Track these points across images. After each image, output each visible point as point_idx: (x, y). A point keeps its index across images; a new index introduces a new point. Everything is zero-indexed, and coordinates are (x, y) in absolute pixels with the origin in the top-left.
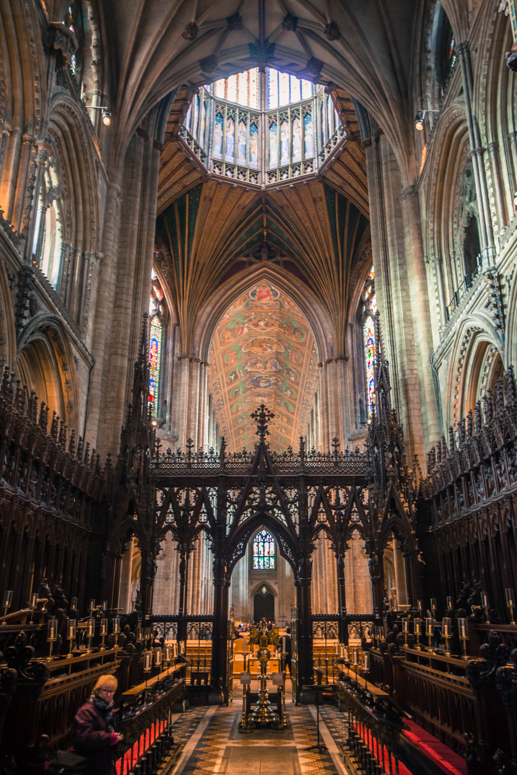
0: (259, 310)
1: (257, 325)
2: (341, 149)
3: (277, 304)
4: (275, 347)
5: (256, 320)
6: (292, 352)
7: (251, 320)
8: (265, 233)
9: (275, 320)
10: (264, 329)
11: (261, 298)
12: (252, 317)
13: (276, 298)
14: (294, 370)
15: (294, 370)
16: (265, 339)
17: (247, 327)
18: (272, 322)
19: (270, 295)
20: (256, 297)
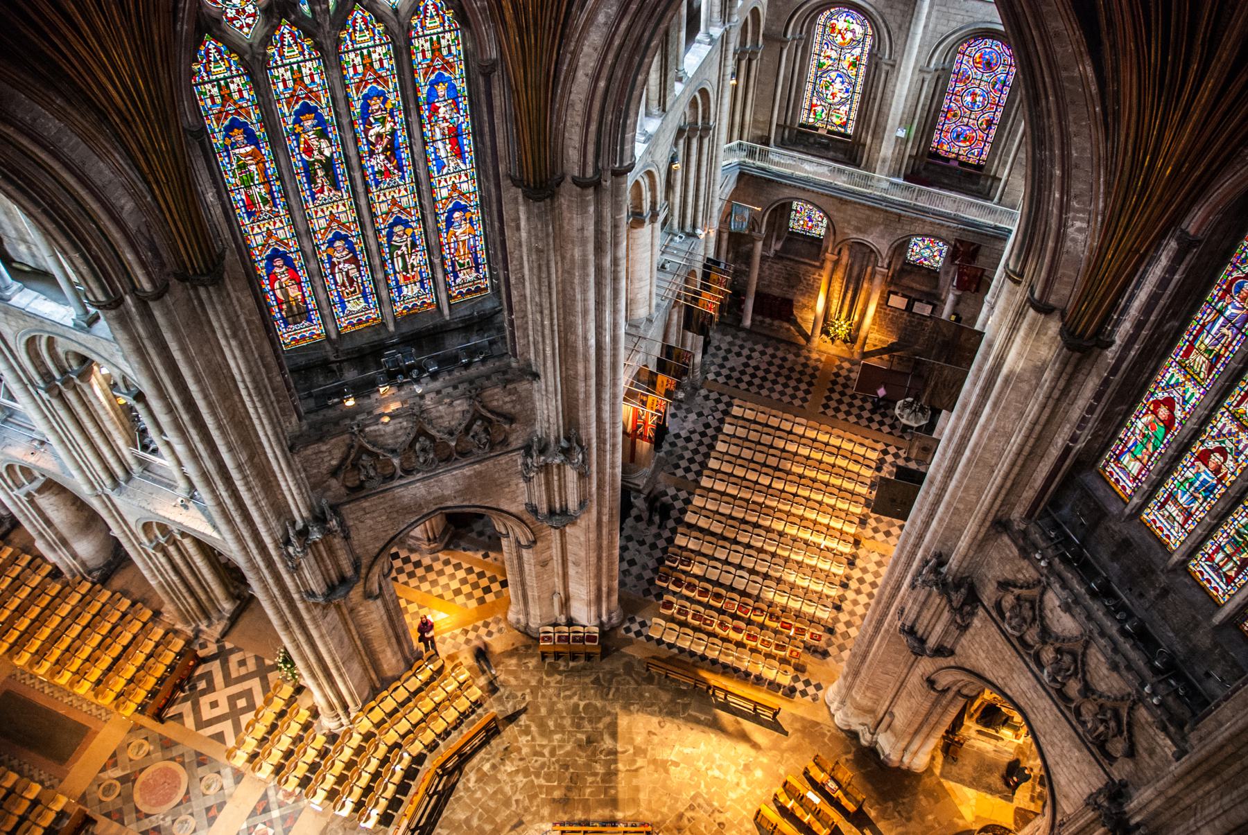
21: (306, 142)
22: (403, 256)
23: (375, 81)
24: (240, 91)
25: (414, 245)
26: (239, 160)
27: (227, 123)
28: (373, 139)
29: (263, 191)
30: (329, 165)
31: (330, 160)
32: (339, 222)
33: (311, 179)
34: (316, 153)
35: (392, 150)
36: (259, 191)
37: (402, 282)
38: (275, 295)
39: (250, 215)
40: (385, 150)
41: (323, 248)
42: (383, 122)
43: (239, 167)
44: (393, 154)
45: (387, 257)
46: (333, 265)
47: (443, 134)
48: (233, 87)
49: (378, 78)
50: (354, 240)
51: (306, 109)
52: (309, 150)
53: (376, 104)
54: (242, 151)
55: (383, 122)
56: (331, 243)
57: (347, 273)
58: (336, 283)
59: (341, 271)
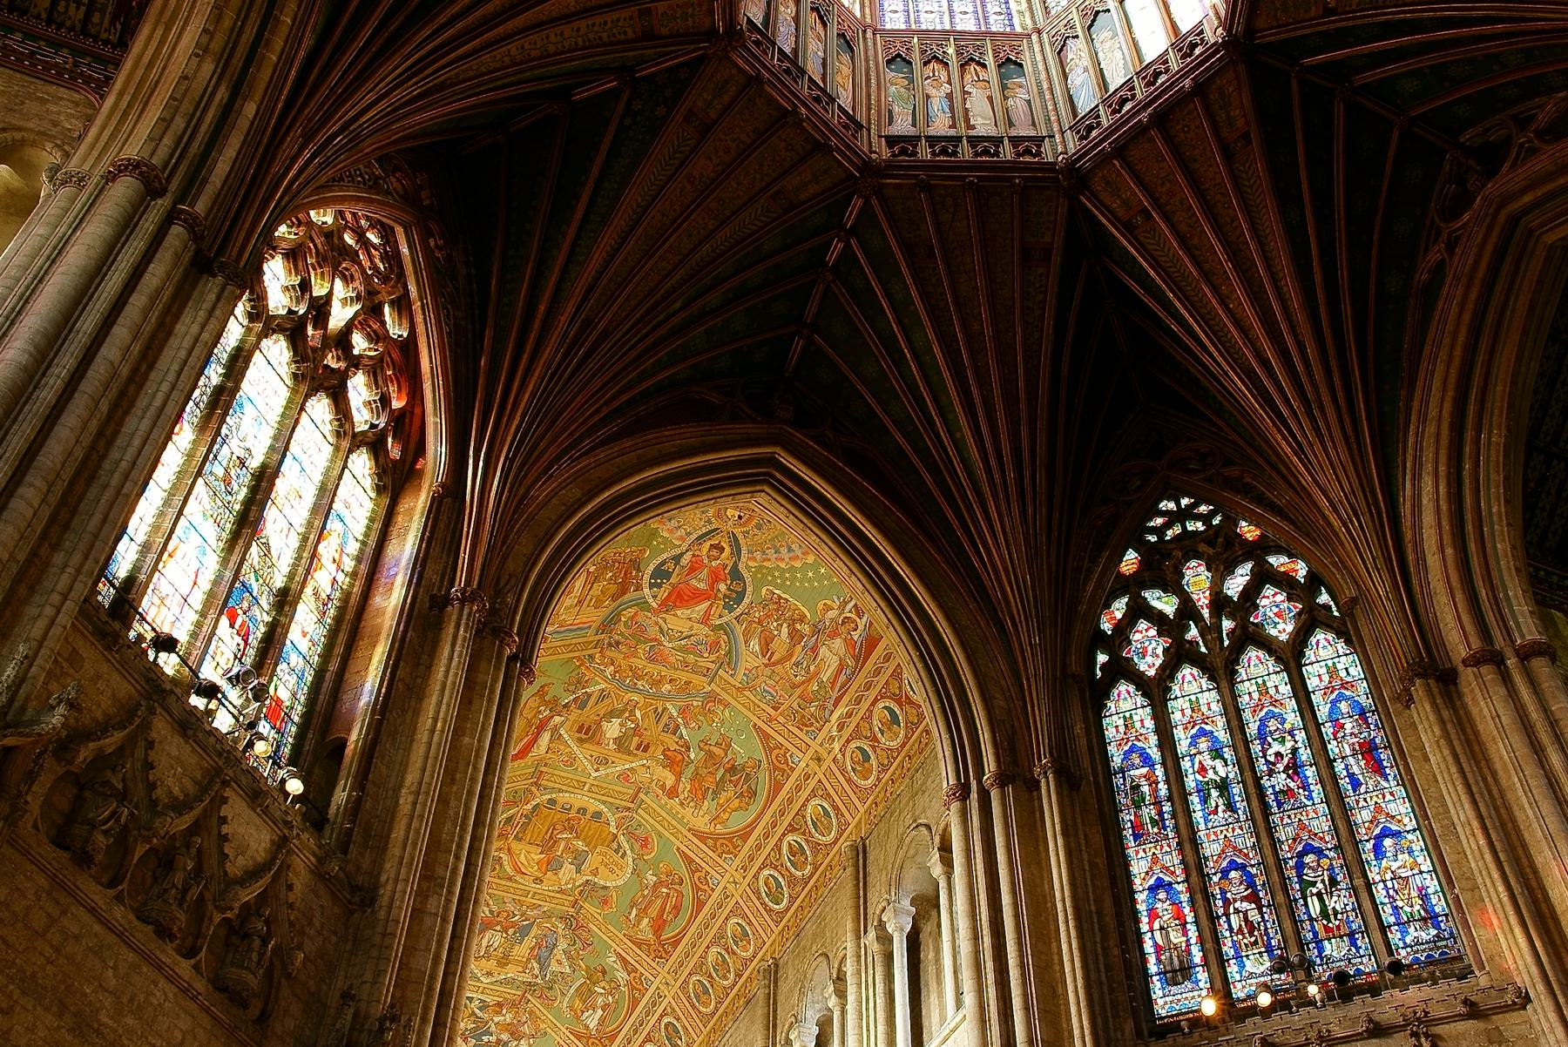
0: (639, 662)
1: (588, 733)
2: (1187, 82)
5: (603, 709)
6: (656, 886)
8: (798, 345)
10: (603, 762)
14: (621, 976)
15: (621, 976)
18: (653, 731)
20: (663, 593)
21: (1200, 762)
22: (1319, 895)
23: (1271, 704)
24: (1142, 721)
25: (1333, 882)
26: (1133, 781)
27: (1126, 748)
28: (1272, 759)
29: (1153, 812)
30: (1223, 786)
31: (1224, 780)
32: (1235, 848)
33: (1205, 800)
34: (1211, 772)
35: (1294, 768)
36: (1148, 812)
37: (1322, 935)
38: (1153, 937)
39: (1136, 837)
40: (1287, 768)
41: (1215, 879)
42: (1282, 741)
43: (1132, 788)
44: (1296, 773)
45: (1298, 896)
46: (1227, 903)
47: (1354, 749)
48: (1136, 718)
49: (1274, 702)
50: (1253, 871)
51: (1203, 733)
52: (1203, 770)
53: (1272, 725)
54: (1137, 772)
55: (1282, 741)
56: (1225, 873)
57: (1245, 914)
58: (1231, 929)
59: (1237, 911)
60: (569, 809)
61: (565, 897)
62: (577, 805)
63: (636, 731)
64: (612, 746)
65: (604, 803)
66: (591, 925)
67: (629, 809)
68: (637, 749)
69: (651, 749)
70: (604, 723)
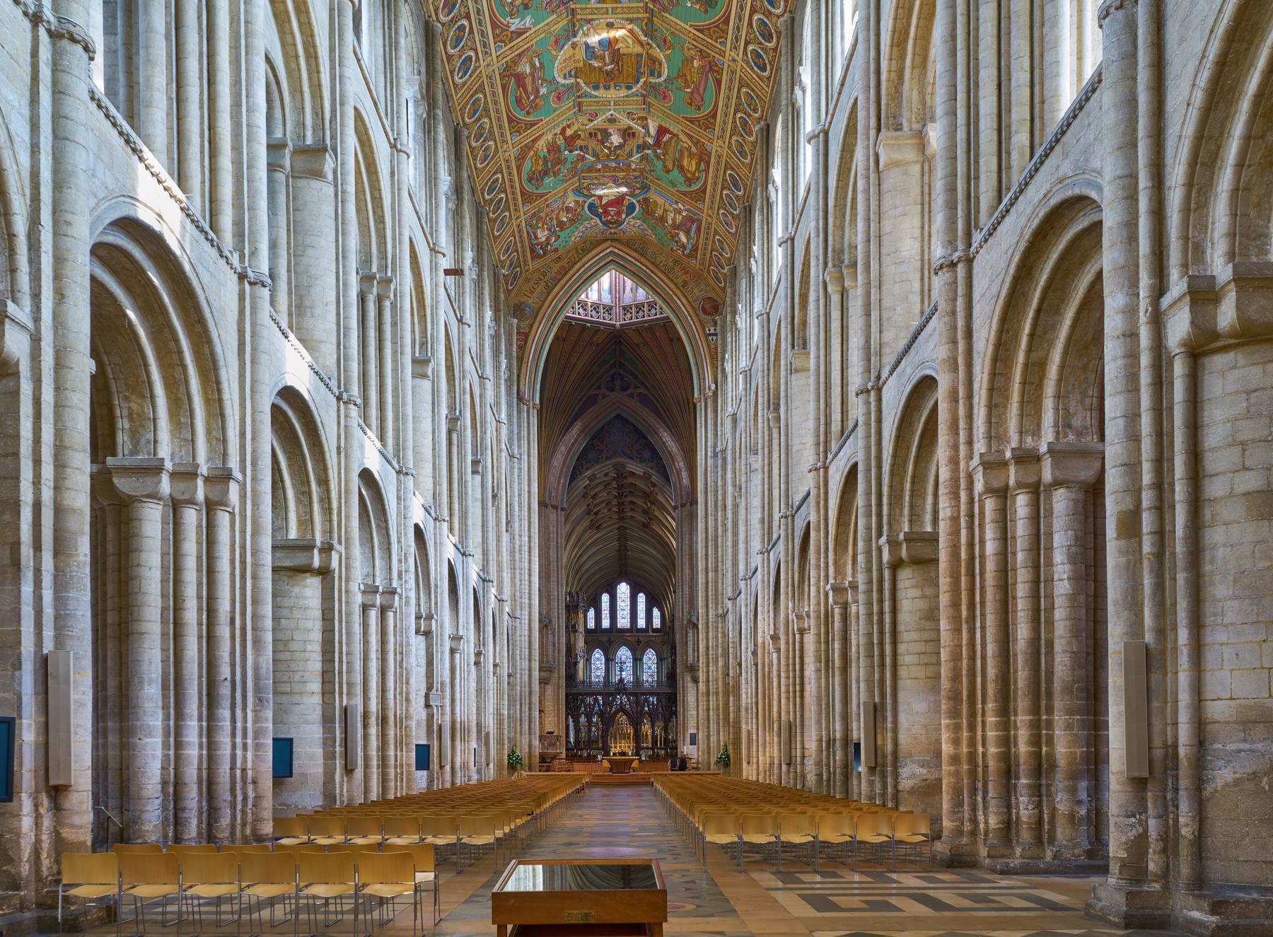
0: (621, 174)
1: (627, 133)
3: (588, 190)
4: (581, 54)
5: (627, 148)
7: (642, 147)
9: (586, 147)
10: (612, 120)
11: (619, 200)
12: (636, 157)
13: (591, 200)
16: (607, 88)
17: (649, 135)
18: (592, 144)
19: (601, 206)
20: (626, 203)
60: (615, 86)
61: (584, 17)
62: (612, 91)
63: (603, 143)
64: (611, 131)
65: (596, 97)
66: (555, 16)
67: (579, 97)
68: (596, 134)
69: (587, 135)
70: (621, 141)
